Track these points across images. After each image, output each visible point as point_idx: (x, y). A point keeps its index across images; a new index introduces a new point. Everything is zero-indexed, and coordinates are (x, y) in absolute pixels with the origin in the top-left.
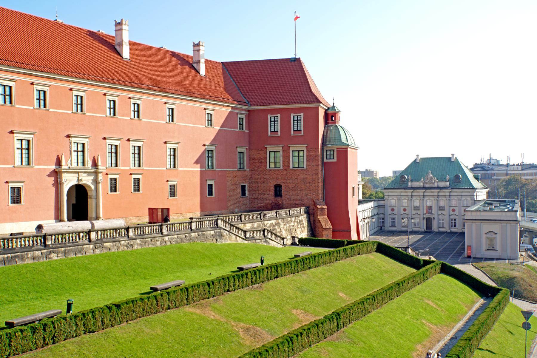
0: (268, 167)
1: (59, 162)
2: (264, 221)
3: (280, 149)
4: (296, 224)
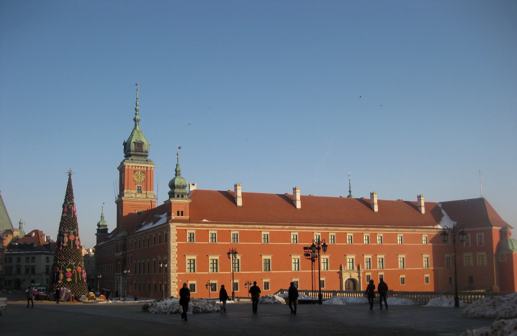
1: (341, 269)
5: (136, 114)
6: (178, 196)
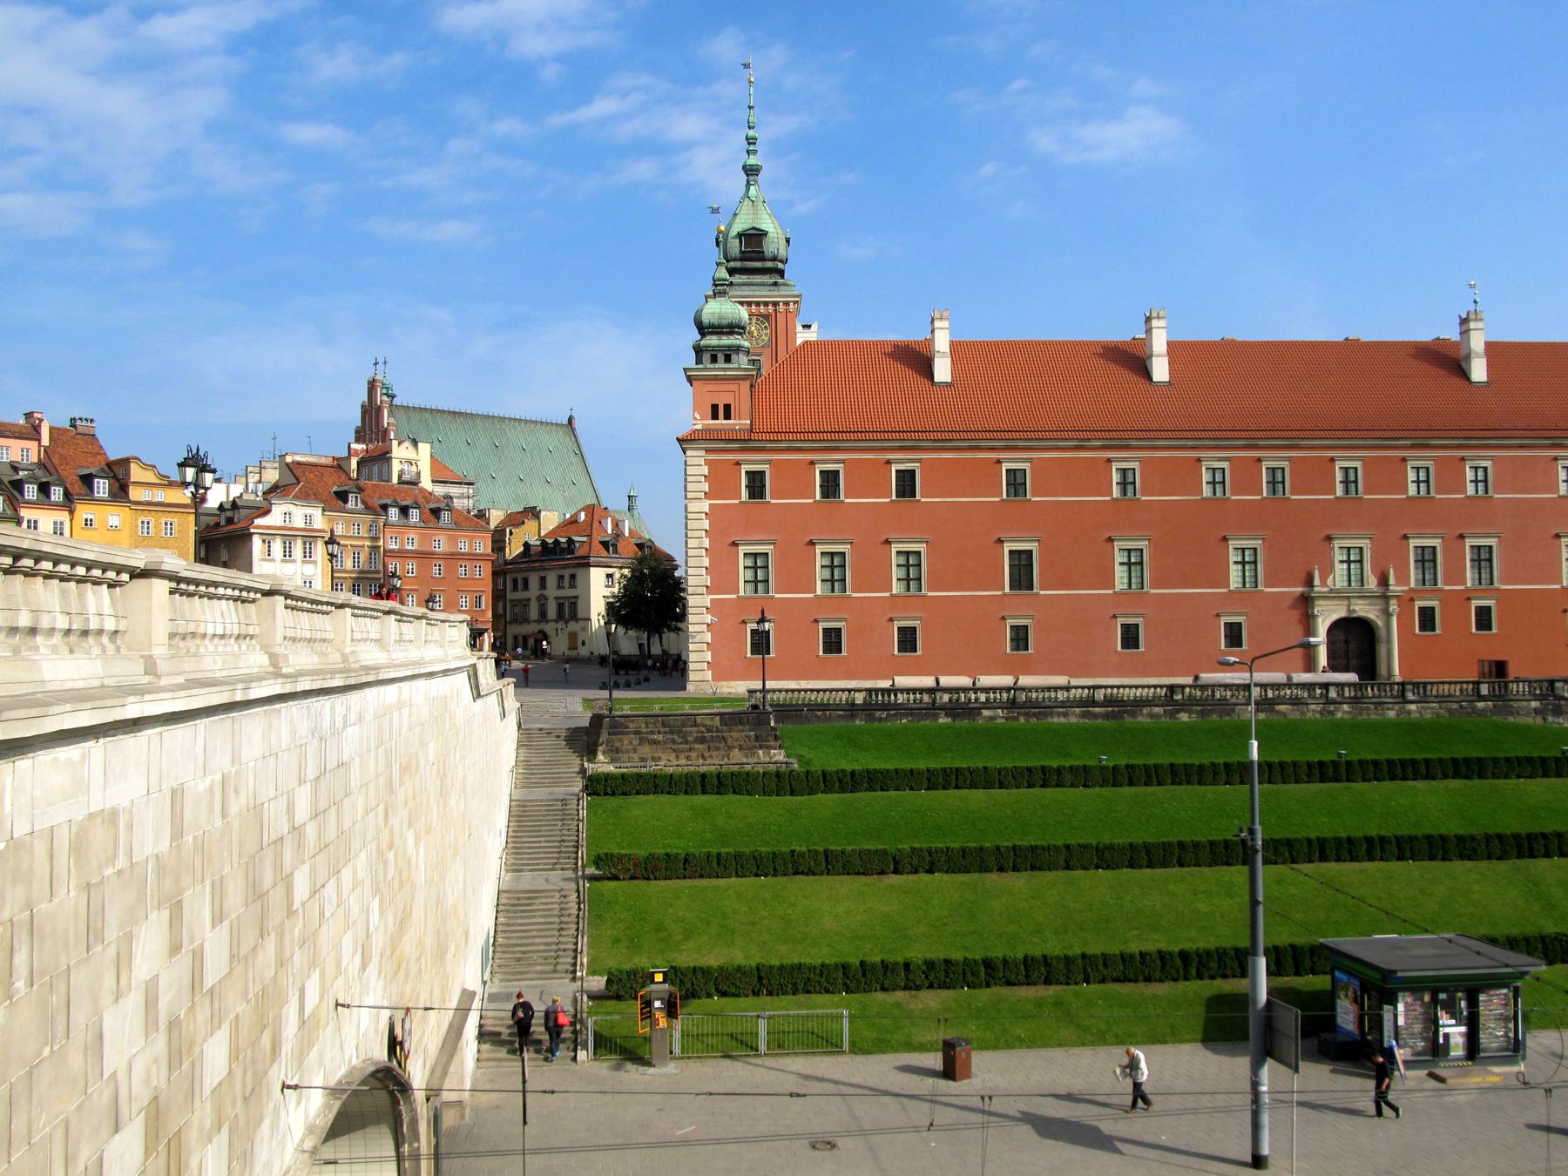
1: (1309, 582)
6: (714, 359)
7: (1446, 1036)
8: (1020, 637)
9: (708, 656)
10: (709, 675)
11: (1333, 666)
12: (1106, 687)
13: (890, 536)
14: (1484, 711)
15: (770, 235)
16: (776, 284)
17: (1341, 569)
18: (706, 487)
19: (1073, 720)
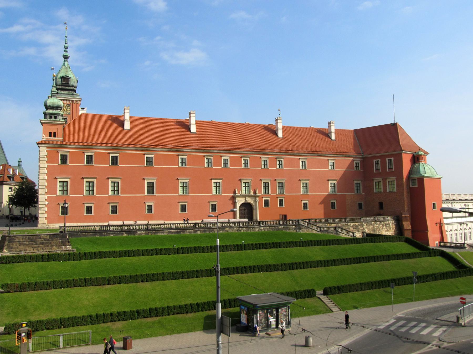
0: (375, 192)
1: (235, 192)
2: (348, 222)
3: (381, 180)
4: (381, 226)
5: (65, 51)
6: (51, 117)
7: (271, 322)
8: (150, 209)
9: (46, 215)
10: (46, 222)
11: (241, 218)
12: (176, 224)
13: (83, 177)
14: (281, 229)
15: (72, 78)
16: (73, 94)
17: (243, 189)
18: (47, 159)
19: (166, 234)
